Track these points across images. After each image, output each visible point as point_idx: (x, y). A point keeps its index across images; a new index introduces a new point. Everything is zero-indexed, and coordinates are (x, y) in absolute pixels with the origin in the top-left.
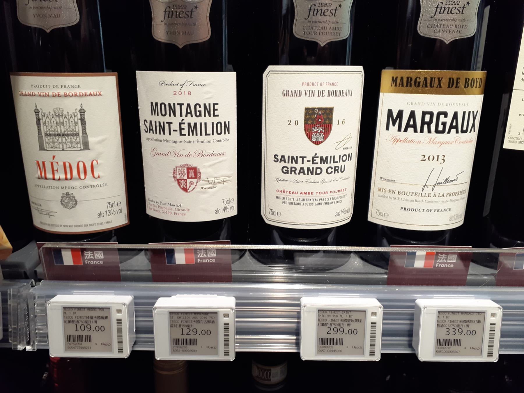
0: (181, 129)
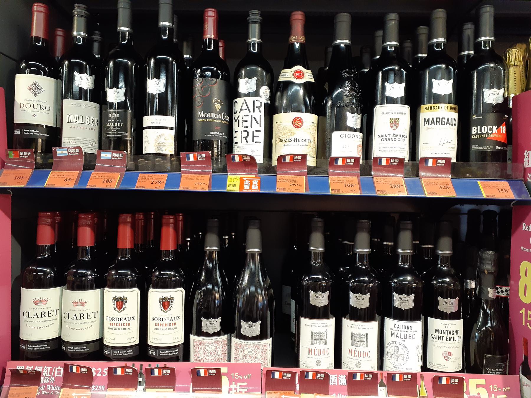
0: (447, 339)
